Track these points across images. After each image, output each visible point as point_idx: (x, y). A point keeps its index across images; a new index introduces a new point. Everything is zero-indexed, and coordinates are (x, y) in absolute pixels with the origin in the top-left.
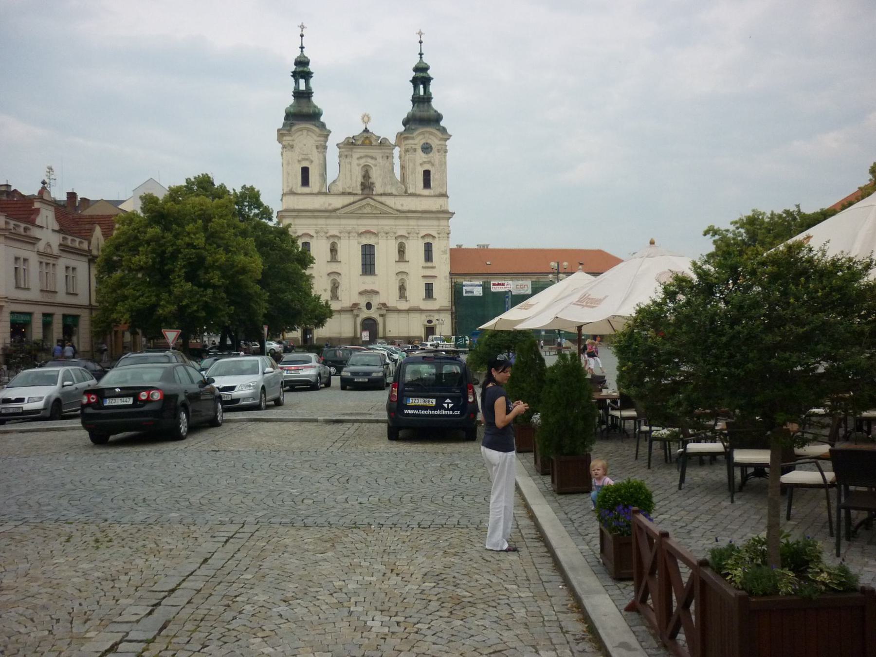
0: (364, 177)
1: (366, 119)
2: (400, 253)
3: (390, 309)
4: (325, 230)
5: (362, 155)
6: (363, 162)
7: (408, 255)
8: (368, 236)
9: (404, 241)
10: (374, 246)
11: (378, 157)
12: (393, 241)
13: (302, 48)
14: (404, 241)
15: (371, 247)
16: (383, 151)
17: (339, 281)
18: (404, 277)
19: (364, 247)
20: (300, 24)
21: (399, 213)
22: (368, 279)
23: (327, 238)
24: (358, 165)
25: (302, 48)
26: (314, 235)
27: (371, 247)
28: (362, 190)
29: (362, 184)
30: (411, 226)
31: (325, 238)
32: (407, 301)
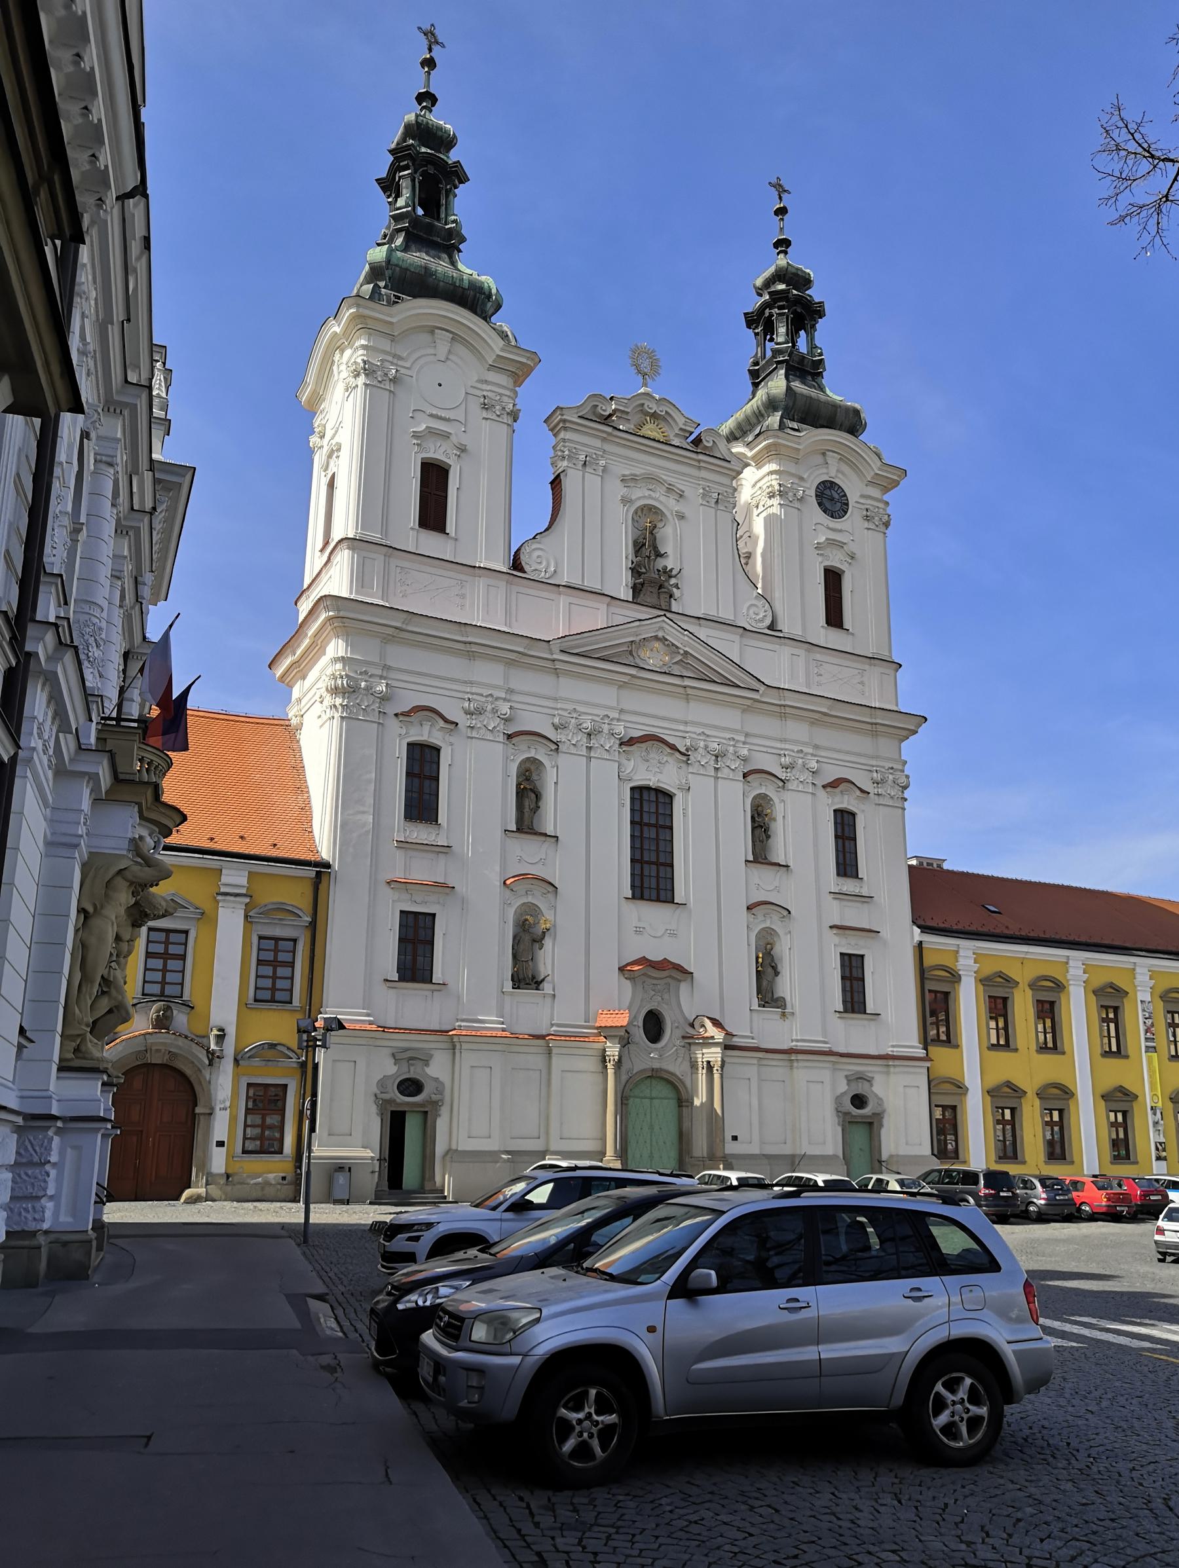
0: (638, 547)
1: (645, 365)
2: (757, 832)
3: (736, 1041)
4: (505, 708)
5: (638, 471)
6: (641, 495)
7: (781, 847)
8: (656, 754)
9: (769, 789)
10: (669, 796)
11: (688, 492)
12: (739, 786)
13: (427, 99)
14: (769, 789)
15: (664, 798)
16: (704, 474)
17: (548, 914)
18: (773, 922)
19: (640, 794)
20: (426, 27)
21: (762, 688)
22: (652, 914)
23: (509, 737)
24: (625, 501)
25: (427, 99)
26: (463, 720)
27: (664, 798)
28: (636, 590)
29: (635, 571)
30: (795, 742)
31: (501, 738)
32: (783, 1015)
